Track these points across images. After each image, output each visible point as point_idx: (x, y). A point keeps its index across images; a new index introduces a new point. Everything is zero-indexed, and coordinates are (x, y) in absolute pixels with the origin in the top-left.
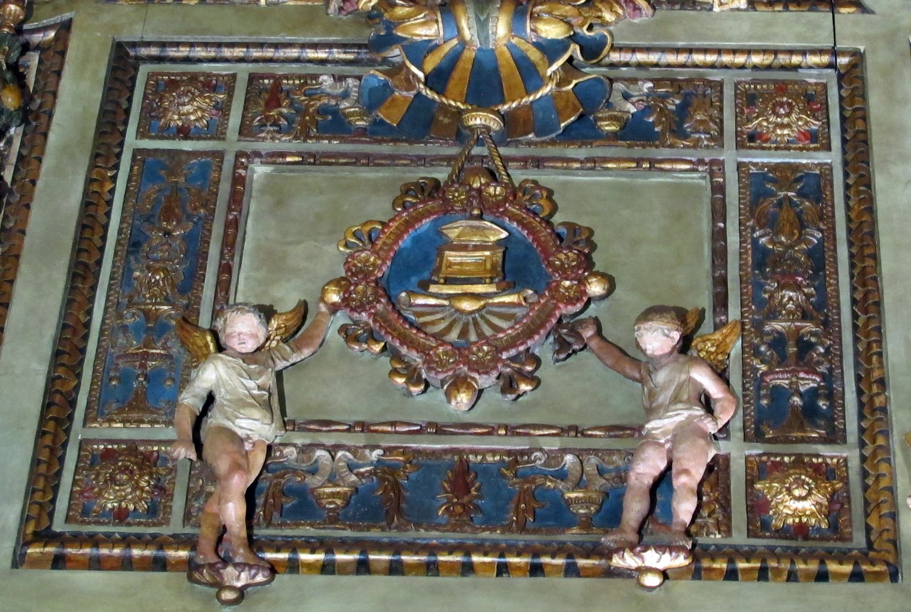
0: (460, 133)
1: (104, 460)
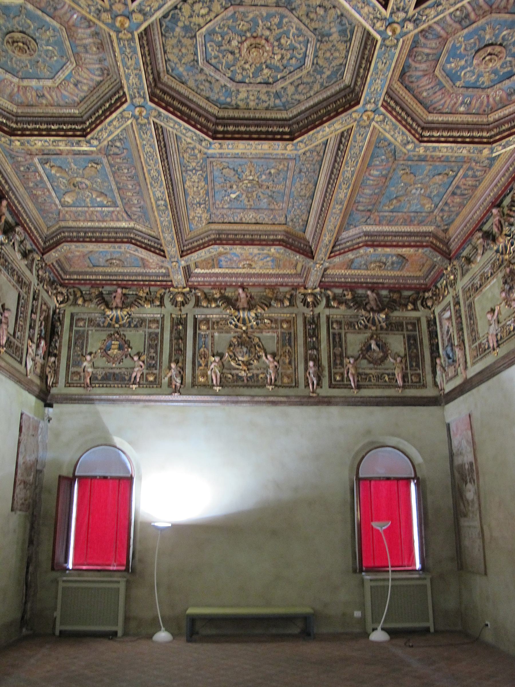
0: (114, 327)
1: (73, 373)
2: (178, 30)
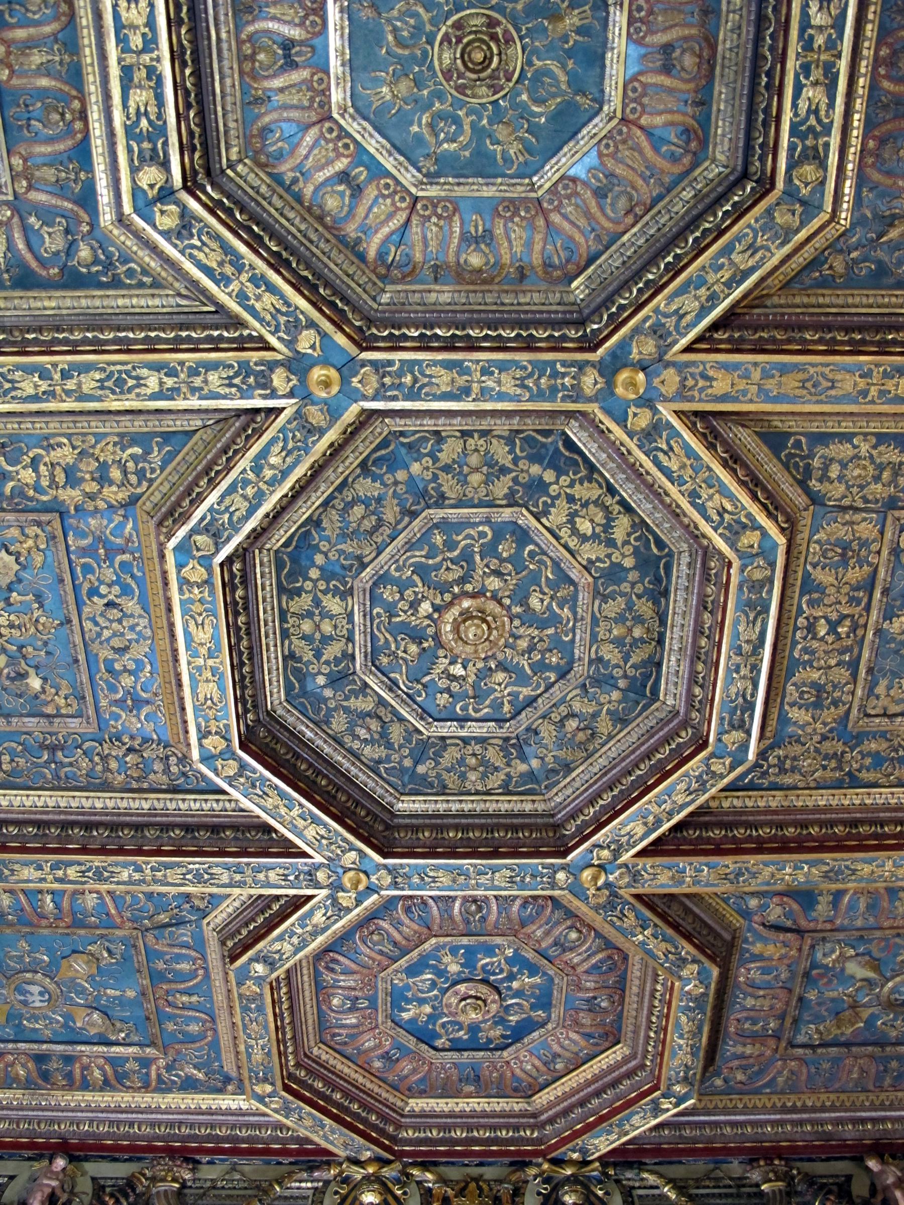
2: (535, 469)
